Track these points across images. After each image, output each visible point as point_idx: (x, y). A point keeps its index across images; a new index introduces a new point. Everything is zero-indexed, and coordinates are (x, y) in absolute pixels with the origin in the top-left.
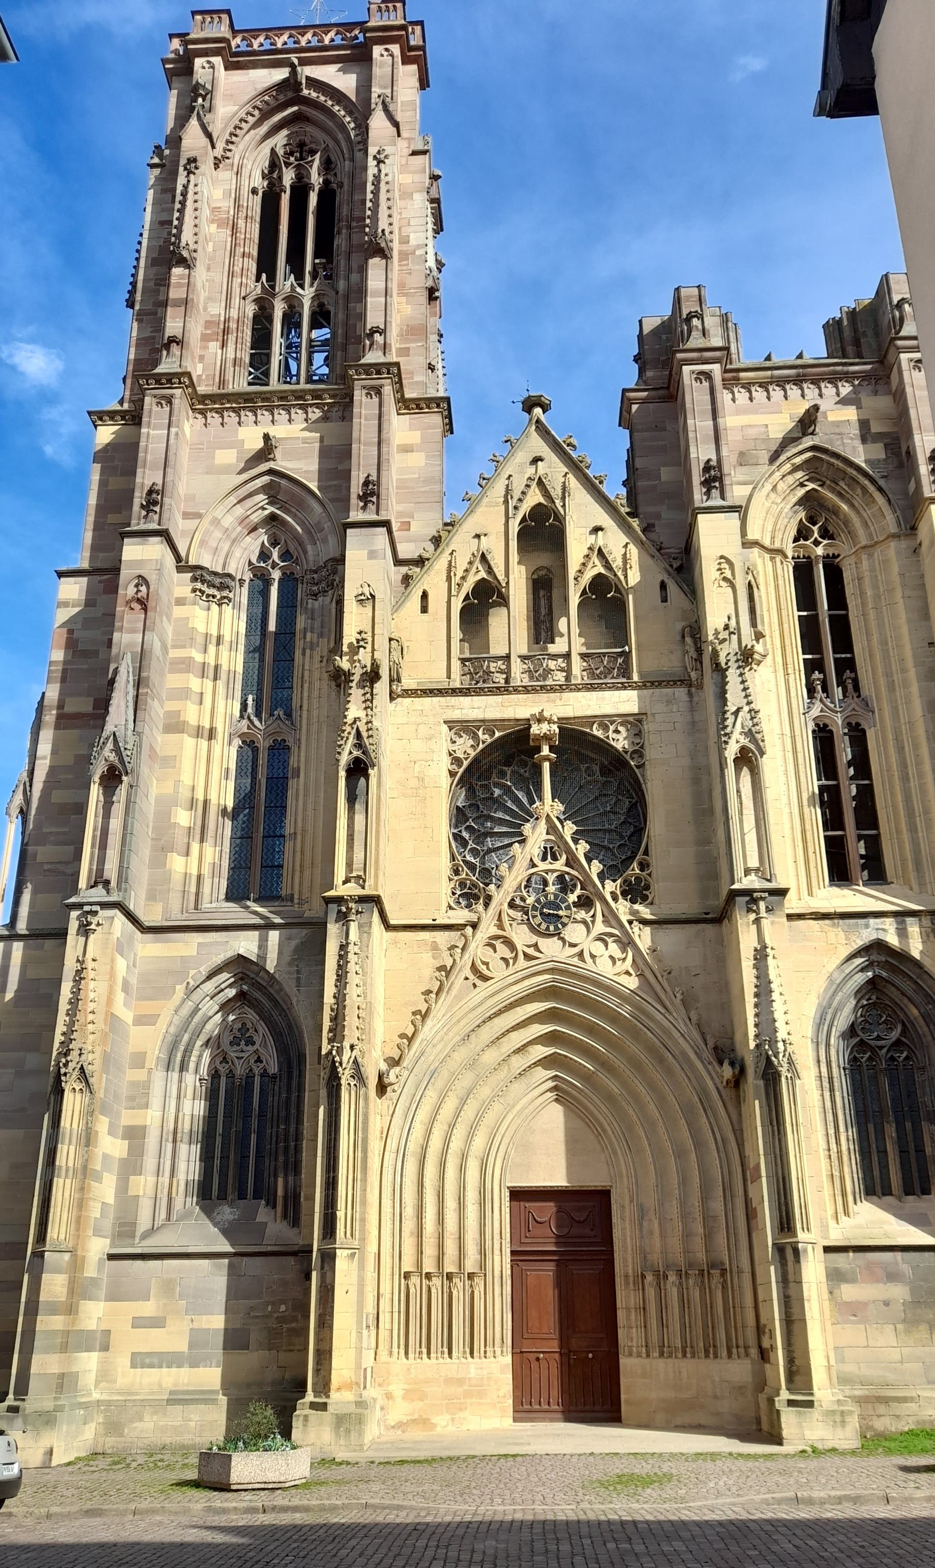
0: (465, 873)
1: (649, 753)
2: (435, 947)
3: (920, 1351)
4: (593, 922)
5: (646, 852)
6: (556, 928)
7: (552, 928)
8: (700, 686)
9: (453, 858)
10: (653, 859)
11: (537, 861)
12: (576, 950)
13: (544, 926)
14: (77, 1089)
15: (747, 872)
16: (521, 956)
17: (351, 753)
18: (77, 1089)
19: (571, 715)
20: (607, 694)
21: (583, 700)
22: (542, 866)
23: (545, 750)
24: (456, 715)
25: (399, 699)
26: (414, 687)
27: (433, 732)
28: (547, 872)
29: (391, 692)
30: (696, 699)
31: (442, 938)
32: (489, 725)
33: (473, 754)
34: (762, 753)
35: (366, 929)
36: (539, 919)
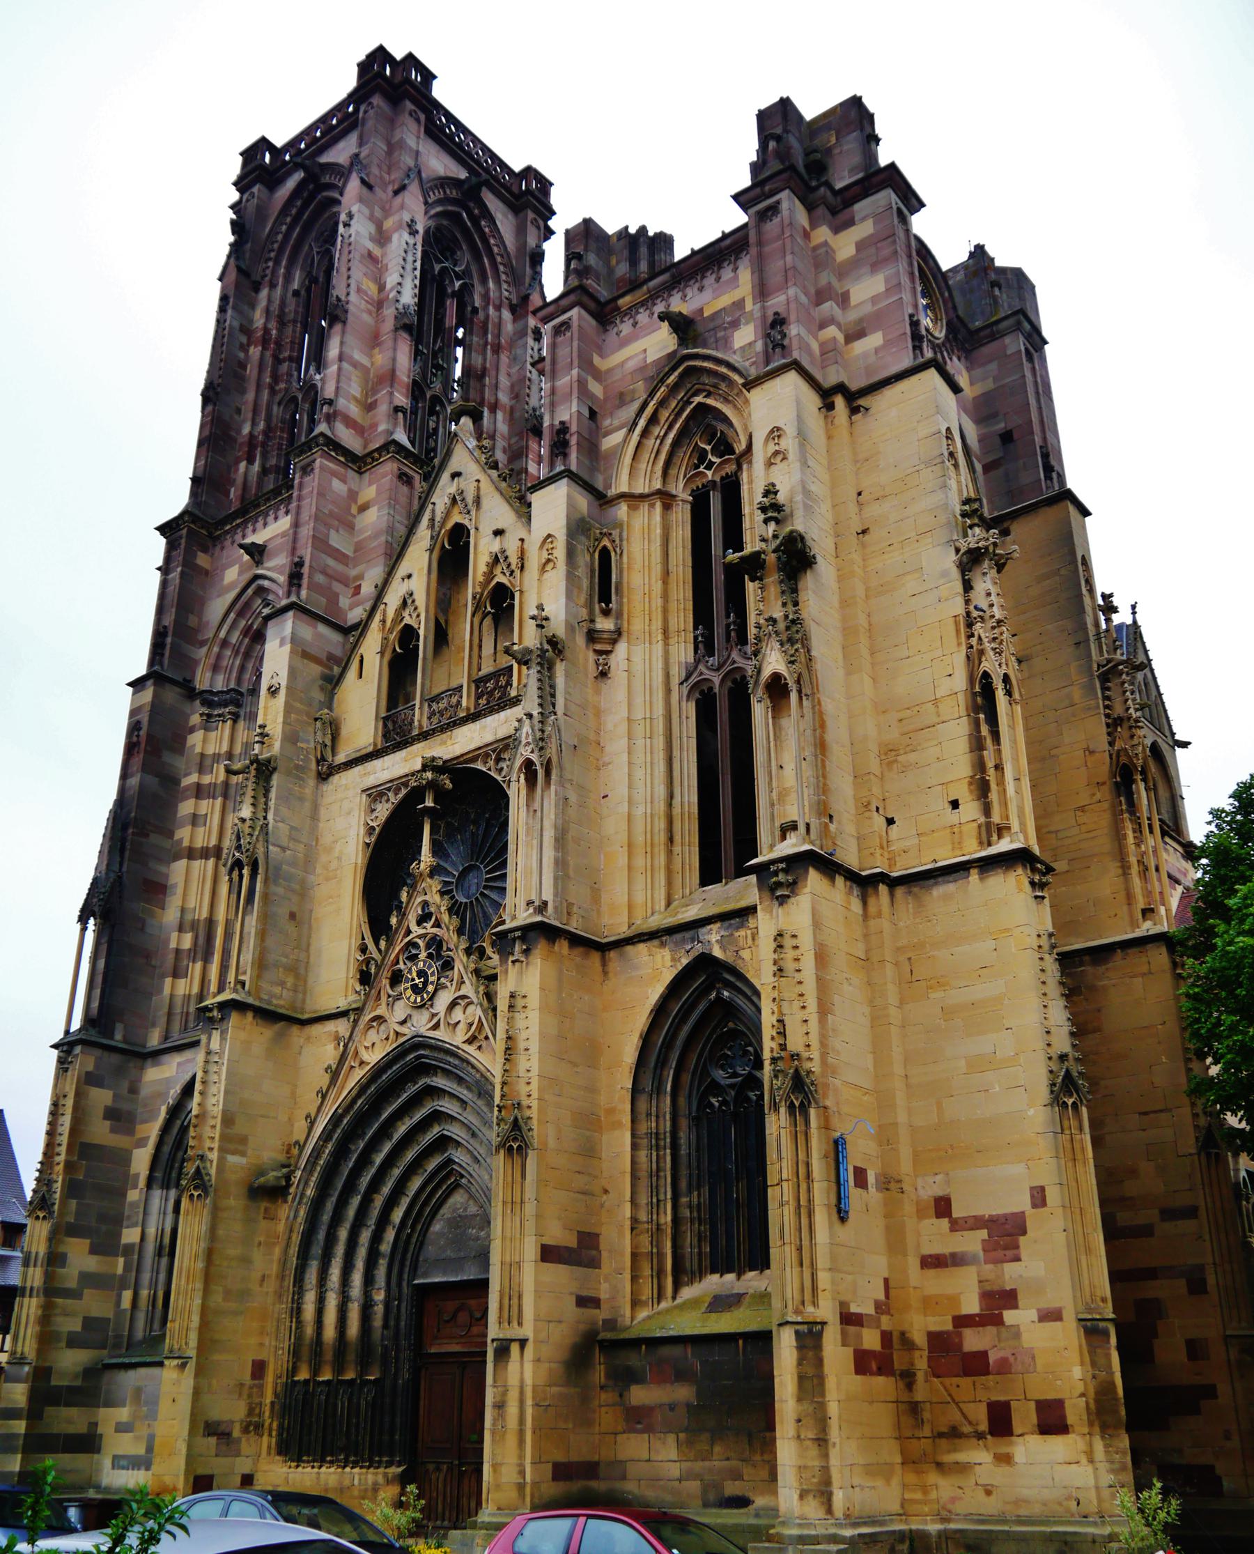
3: (698, 1466)
14: (41, 1215)
18: (41, 1215)
19: (458, 753)
23: (429, 803)
24: (371, 781)
32: (397, 784)
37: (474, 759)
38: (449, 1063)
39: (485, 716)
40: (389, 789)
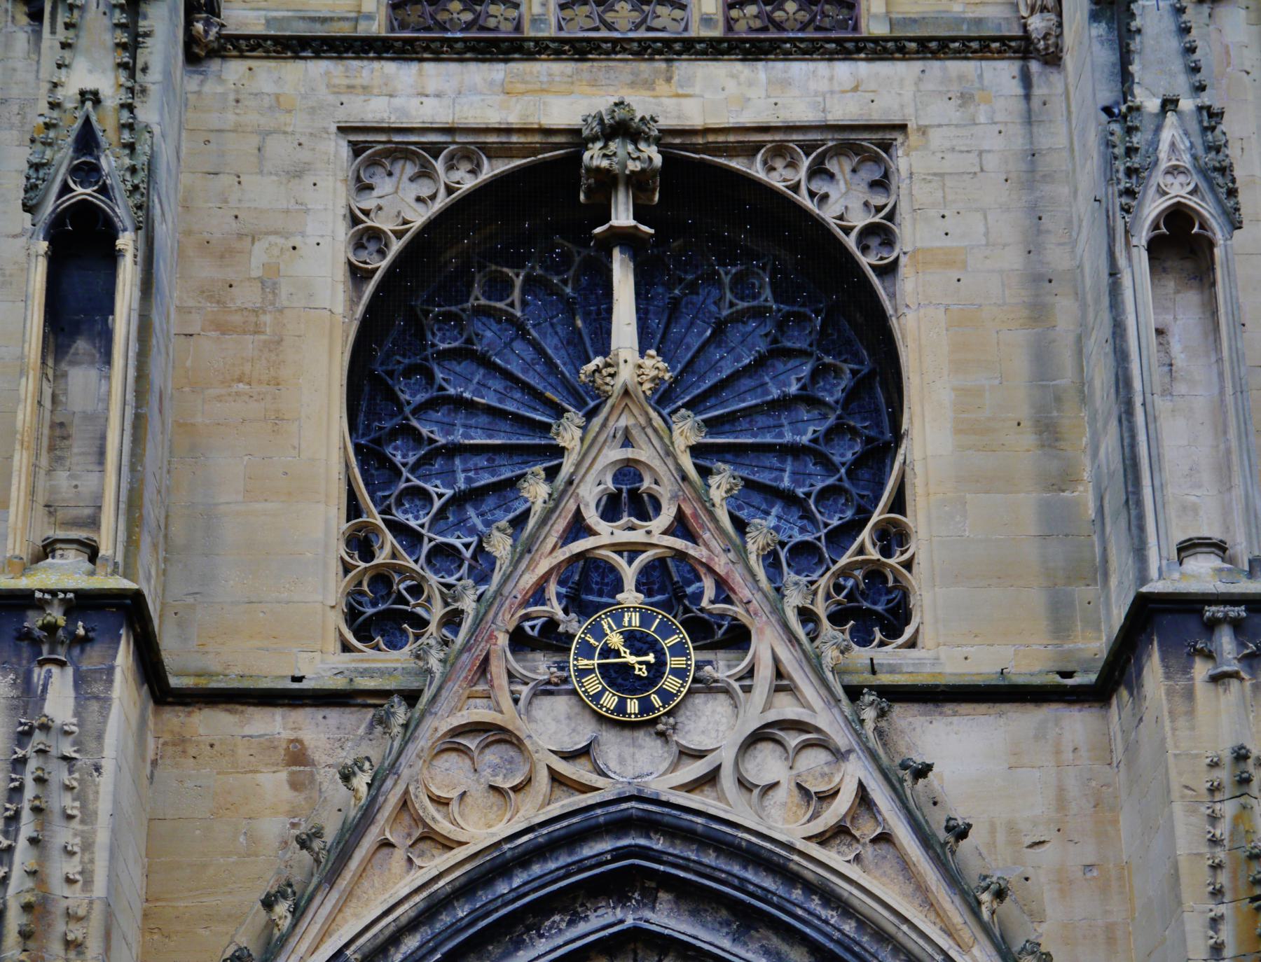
0: (387, 548)
1: (909, 234)
2: (297, 756)
4: (747, 690)
5: (899, 504)
6: (646, 707)
7: (633, 706)
8: (1053, 59)
9: (354, 509)
10: (917, 519)
11: (592, 517)
12: (695, 769)
13: (610, 700)
15: (1188, 548)
16: (543, 778)
17: (65, 189)
19: (697, 122)
20: (798, 69)
21: (731, 86)
22: (607, 534)
23: (622, 216)
24: (375, 110)
25: (215, 65)
26: (259, 30)
27: (304, 155)
28: (619, 548)
29: (191, 41)
30: (1039, 91)
31: (316, 730)
32: (467, 144)
33: (419, 217)
34: (1234, 222)
35: (97, 688)
36: (594, 684)
37: (750, 151)
38: (742, 885)
39: (787, 56)
40: (435, 150)
